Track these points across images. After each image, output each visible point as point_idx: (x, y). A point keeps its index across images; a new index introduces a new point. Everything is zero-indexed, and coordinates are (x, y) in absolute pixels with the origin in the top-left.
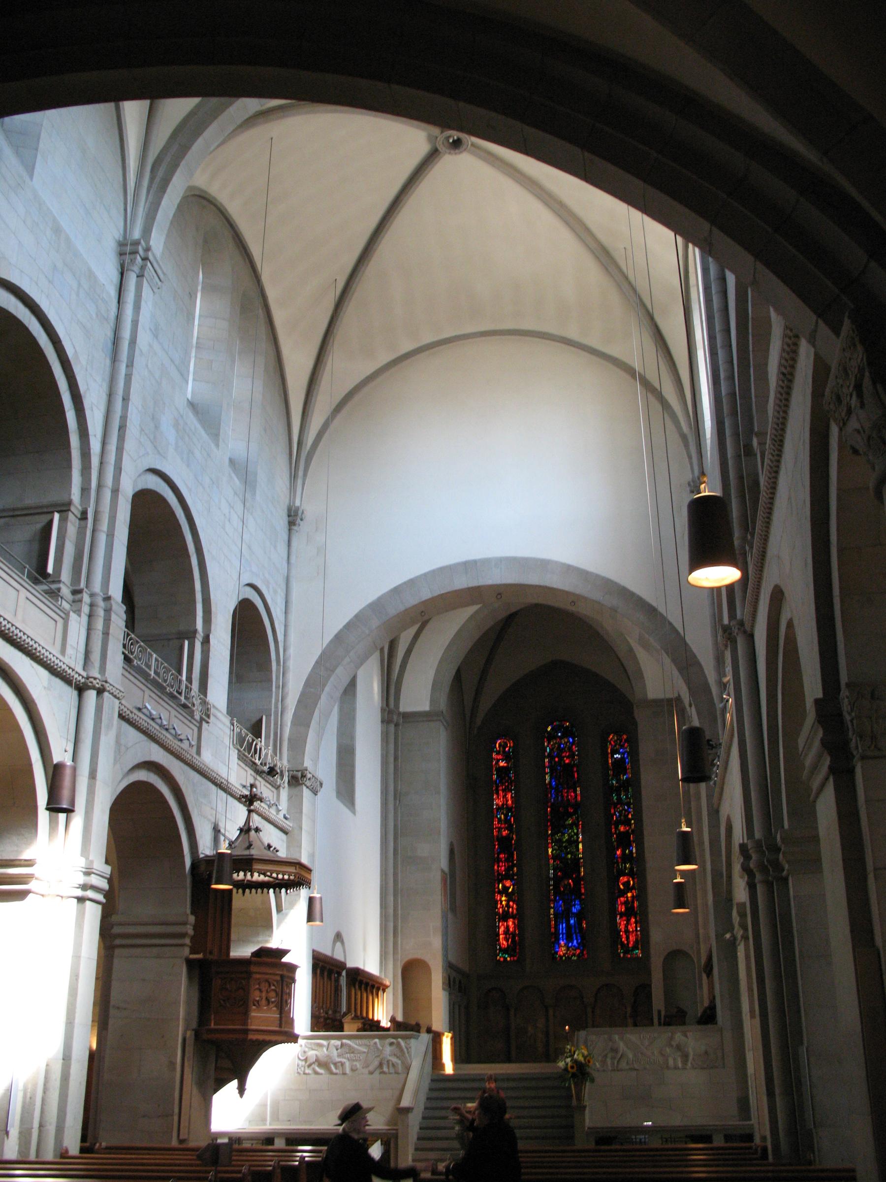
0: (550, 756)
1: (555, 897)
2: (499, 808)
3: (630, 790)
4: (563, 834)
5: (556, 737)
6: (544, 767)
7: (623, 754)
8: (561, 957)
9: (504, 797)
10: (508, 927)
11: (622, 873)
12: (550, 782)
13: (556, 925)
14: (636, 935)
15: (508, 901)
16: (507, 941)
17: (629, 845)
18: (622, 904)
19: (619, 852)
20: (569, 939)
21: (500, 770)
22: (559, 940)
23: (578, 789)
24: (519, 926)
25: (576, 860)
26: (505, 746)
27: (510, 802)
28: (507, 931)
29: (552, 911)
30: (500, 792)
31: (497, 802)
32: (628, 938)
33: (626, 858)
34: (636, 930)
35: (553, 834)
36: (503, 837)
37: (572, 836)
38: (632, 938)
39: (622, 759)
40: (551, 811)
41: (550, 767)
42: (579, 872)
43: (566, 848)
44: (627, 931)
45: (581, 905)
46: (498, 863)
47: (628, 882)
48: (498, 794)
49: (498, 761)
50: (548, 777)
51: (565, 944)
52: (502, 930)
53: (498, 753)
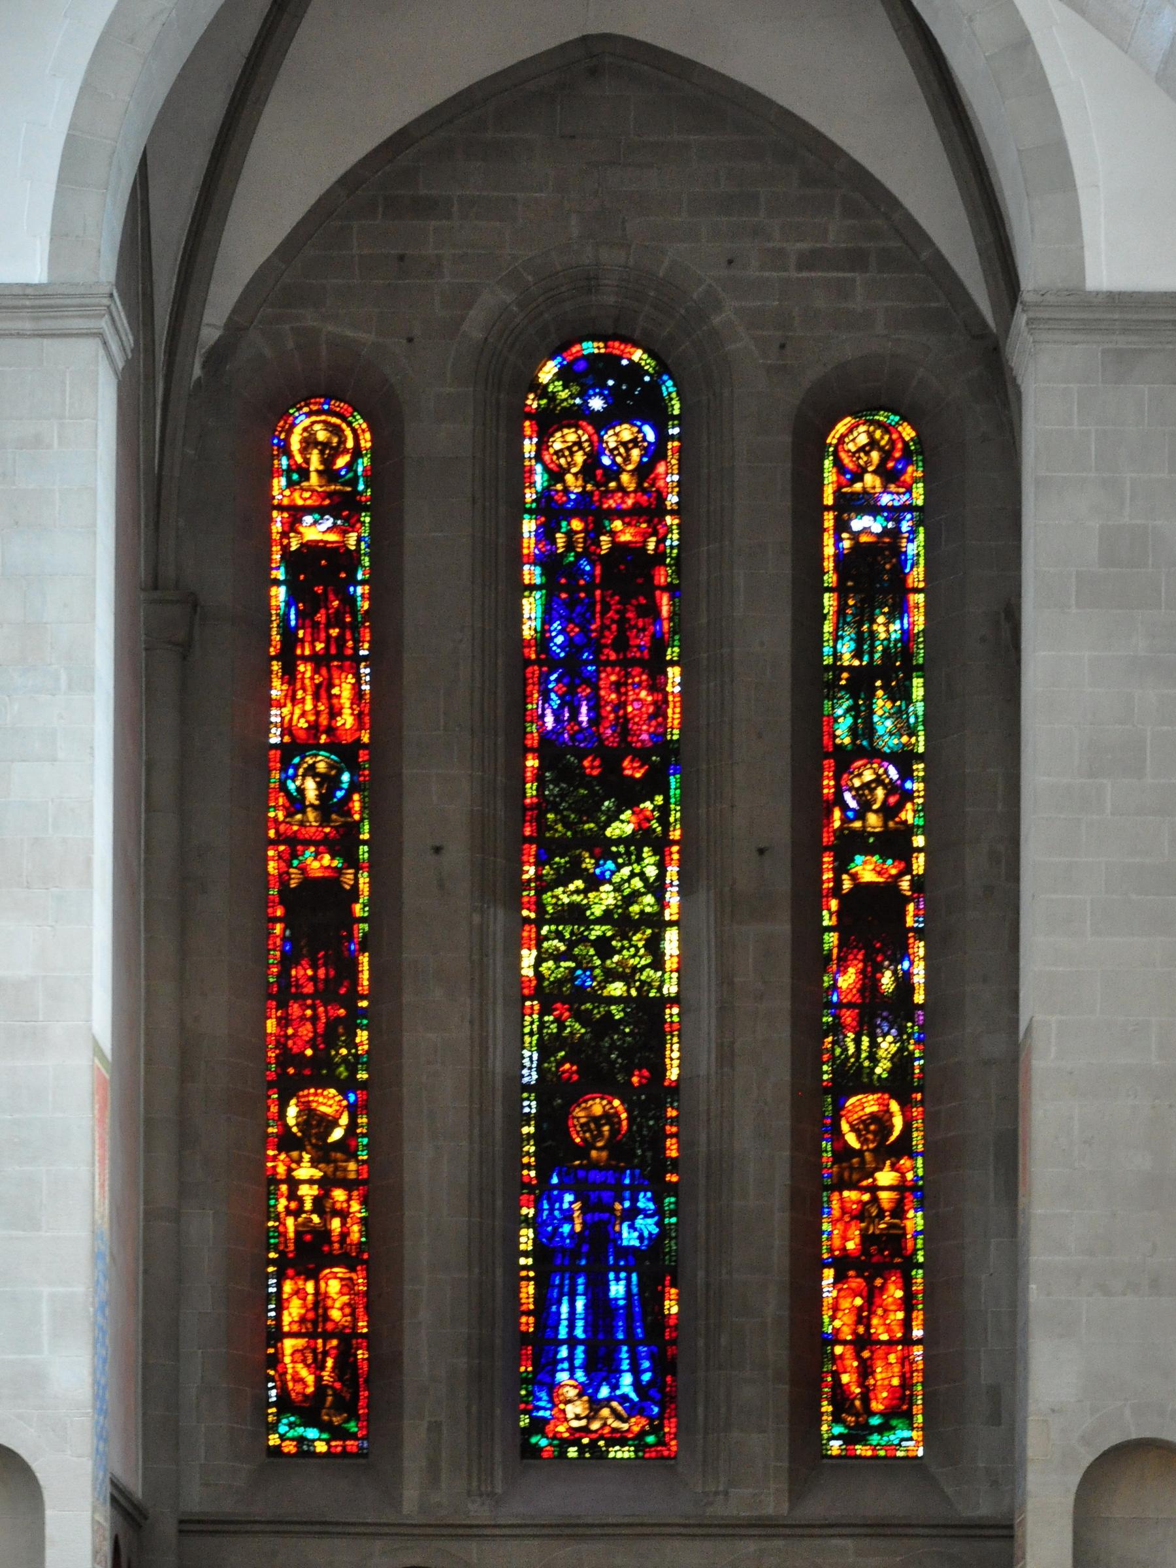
1: (544, 1176)
3: (918, 692)
4: (594, 882)
5: (575, 416)
6: (517, 560)
9: (323, 691)
10: (321, 1299)
11: (853, 1079)
12: (543, 640)
15: (325, 1185)
16: (317, 1366)
19: (848, 980)
20: (601, 1368)
22: (552, 1365)
23: (674, 673)
24: (376, 1301)
25: (647, 1010)
27: (347, 720)
28: (316, 1321)
29: (526, 1239)
31: (287, 713)
32: (865, 1371)
33: (875, 1010)
34: (908, 1341)
36: (309, 882)
37: (634, 896)
38: (886, 1375)
41: (548, 561)
43: (604, 947)
45: (659, 1212)
47: (881, 1121)
48: (289, 675)
49: (296, 514)
50: (532, 607)
52: (294, 1311)
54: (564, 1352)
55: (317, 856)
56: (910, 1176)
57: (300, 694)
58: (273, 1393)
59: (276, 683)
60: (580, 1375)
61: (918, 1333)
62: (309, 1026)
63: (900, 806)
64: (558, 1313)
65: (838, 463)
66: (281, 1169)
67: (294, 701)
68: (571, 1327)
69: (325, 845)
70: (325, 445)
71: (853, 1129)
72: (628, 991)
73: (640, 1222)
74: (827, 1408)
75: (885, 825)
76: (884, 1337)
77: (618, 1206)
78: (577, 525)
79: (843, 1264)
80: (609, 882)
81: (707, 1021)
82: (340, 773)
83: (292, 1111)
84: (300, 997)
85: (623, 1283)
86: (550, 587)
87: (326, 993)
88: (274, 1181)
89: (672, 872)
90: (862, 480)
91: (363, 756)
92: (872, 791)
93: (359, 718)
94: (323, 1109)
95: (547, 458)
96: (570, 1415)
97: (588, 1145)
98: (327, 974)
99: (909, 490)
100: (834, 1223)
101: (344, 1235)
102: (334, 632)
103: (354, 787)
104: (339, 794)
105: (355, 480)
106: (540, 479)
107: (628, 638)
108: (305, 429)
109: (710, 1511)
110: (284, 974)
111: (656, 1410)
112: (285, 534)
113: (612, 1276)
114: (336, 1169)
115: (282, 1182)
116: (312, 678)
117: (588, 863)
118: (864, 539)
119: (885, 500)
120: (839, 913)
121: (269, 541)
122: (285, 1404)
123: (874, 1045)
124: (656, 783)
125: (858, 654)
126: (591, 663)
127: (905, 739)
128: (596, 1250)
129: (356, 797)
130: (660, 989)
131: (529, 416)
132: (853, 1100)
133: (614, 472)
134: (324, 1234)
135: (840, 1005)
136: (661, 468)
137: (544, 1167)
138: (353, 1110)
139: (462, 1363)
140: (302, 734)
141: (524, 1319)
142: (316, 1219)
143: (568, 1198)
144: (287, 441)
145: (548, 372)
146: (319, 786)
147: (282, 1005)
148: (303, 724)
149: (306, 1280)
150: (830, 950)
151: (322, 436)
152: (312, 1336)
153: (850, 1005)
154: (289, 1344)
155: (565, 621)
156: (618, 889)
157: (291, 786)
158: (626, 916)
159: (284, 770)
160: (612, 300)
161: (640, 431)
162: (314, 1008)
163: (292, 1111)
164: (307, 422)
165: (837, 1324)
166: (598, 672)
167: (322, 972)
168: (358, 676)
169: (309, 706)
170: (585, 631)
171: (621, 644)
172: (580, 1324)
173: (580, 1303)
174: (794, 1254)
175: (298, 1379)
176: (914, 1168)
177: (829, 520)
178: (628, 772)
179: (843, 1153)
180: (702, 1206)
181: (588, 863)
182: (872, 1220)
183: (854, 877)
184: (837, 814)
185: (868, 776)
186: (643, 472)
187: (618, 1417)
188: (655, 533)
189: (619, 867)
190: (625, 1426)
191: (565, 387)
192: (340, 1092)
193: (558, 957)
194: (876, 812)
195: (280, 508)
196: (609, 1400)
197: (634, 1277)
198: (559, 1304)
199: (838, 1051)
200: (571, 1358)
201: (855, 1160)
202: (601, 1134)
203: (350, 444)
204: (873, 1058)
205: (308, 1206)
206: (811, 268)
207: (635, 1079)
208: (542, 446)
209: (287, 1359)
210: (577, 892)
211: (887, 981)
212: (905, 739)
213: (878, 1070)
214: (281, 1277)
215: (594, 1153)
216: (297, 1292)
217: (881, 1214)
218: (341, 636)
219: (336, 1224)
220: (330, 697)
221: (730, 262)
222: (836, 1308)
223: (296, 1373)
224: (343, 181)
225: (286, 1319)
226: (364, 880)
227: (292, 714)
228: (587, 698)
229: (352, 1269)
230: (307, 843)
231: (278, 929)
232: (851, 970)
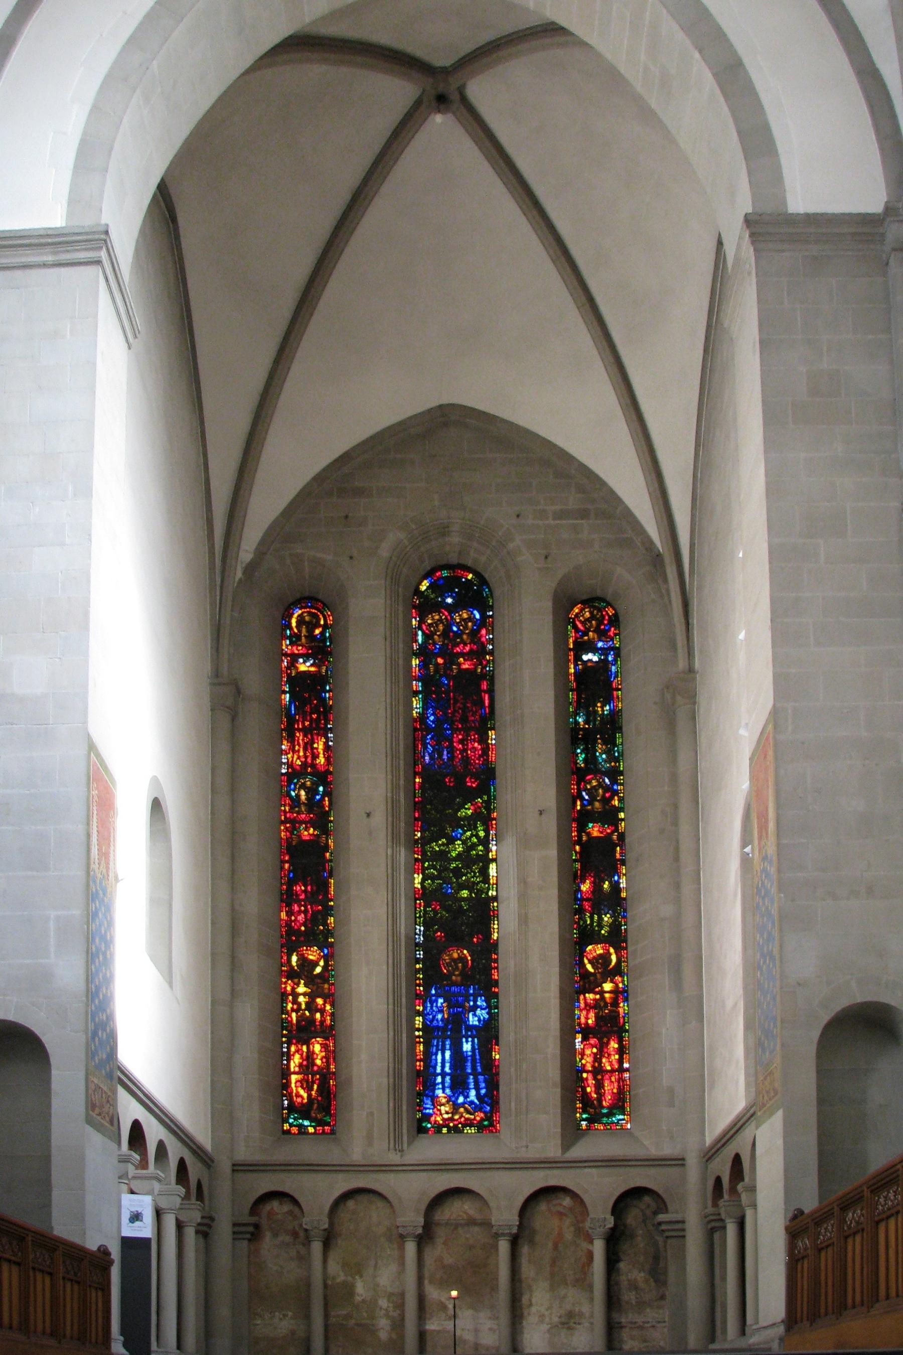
0: (424, 653)
1: (427, 990)
2: (294, 774)
4: (451, 840)
5: (439, 607)
8: (438, 1128)
9: (309, 746)
11: (587, 936)
12: (423, 717)
13: (428, 1056)
14: (620, 1080)
15: (312, 996)
16: (309, 1089)
18: (588, 1007)
20: (459, 1086)
21: (299, 682)
27: (321, 760)
29: (419, 1021)
32: (599, 1086)
34: (621, 1070)
35: (425, 841)
36: (302, 842)
37: (474, 846)
38: (610, 1087)
39: (603, 665)
40: (422, 785)
43: (457, 872)
44: (598, 1071)
45: (489, 1007)
46: (289, 905)
47: (606, 957)
48: (292, 739)
49: (294, 658)
51: (449, 1099)
53: (295, 639)
54: (439, 1079)
55: (306, 829)
56: (621, 985)
57: (297, 748)
58: (286, 1102)
59: (285, 742)
60: (448, 1091)
61: (626, 1065)
62: (303, 915)
63: (612, 798)
64: (436, 1060)
65: (575, 627)
66: (289, 988)
67: (294, 752)
68: (443, 1066)
69: (309, 823)
71: (590, 962)
72: (471, 894)
73: (478, 1012)
75: (604, 807)
76: (609, 1068)
77: (467, 1004)
78: (440, 661)
79: (587, 1032)
80: (460, 840)
82: (318, 786)
83: (294, 959)
84: (298, 902)
85: (470, 1043)
88: (284, 995)
90: (587, 635)
92: (597, 790)
93: (328, 759)
94: (311, 957)
95: (424, 627)
96: (443, 1112)
97: (450, 974)
98: (312, 888)
99: (612, 640)
100: (581, 1010)
101: (323, 1021)
102: (314, 716)
104: (318, 797)
105: (324, 641)
106: (420, 638)
107: (467, 717)
108: (299, 616)
111: (489, 1108)
112: (288, 668)
113: (464, 1040)
114: (318, 987)
115: (290, 995)
116: (303, 740)
117: (449, 830)
118: (589, 664)
119: (600, 644)
120: (581, 853)
123: (600, 919)
125: (587, 722)
126: (449, 729)
127: (613, 764)
128: (456, 1027)
129: (327, 799)
130: (487, 893)
132: (590, 947)
134: (312, 1020)
135: (582, 899)
136: (484, 632)
138: (327, 958)
140: (298, 768)
141: (418, 1063)
142: (307, 1013)
143: (441, 1001)
144: (290, 623)
145: (424, 586)
146: (307, 794)
147: (289, 905)
149: (302, 1045)
150: (576, 872)
153: (587, 900)
154: (294, 1078)
157: (293, 794)
161: (472, 613)
162: (305, 906)
163: (294, 959)
164: (300, 612)
165: (583, 1062)
166: (452, 734)
167: (309, 888)
168: (327, 739)
169: (301, 754)
170: (445, 714)
171: (464, 720)
172: (447, 1065)
173: (448, 1054)
175: (298, 1095)
176: (623, 982)
178: (469, 784)
179: (585, 974)
182: (601, 1008)
183: (588, 834)
184: (579, 803)
185: (594, 783)
187: (468, 1112)
188: (481, 664)
189: (465, 832)
190: (472, 1117)
191: (432, 593)
192: (319, 948)
193: (433, 878)
194: (598, 801)
195: (286, 655)
196: (464, 1103)
197: (476, 1040)
198: (436, 1054)
199: (581, 923)
200: (443, 1083)
201: (592, 978)
202: (457, 968)
203: (322, 622)
204: (601, 926)
205: (303, 1006)
206: (560, 518)
207: (475, 940)
208: (421, 622)
209: (293, 1085)
210: (443, 844)
211: (606, 885)
212: (613, 764)
213: (603, 932)
215: (454, 978)
216: (297, 1051)
217: (606, 1004)
218: (318, 718)
219: (318, 1016)
220: (313, 748)
221: (518, 516)
222: (583, 1054)
223: (297, 1092)
224: (314, 479)
225: (292, 1065)
227: (293, 757)
228: (447, 748)
229: (327, 1039)
230: (301, 823)
231: (287, 866)
232: (588, 881)
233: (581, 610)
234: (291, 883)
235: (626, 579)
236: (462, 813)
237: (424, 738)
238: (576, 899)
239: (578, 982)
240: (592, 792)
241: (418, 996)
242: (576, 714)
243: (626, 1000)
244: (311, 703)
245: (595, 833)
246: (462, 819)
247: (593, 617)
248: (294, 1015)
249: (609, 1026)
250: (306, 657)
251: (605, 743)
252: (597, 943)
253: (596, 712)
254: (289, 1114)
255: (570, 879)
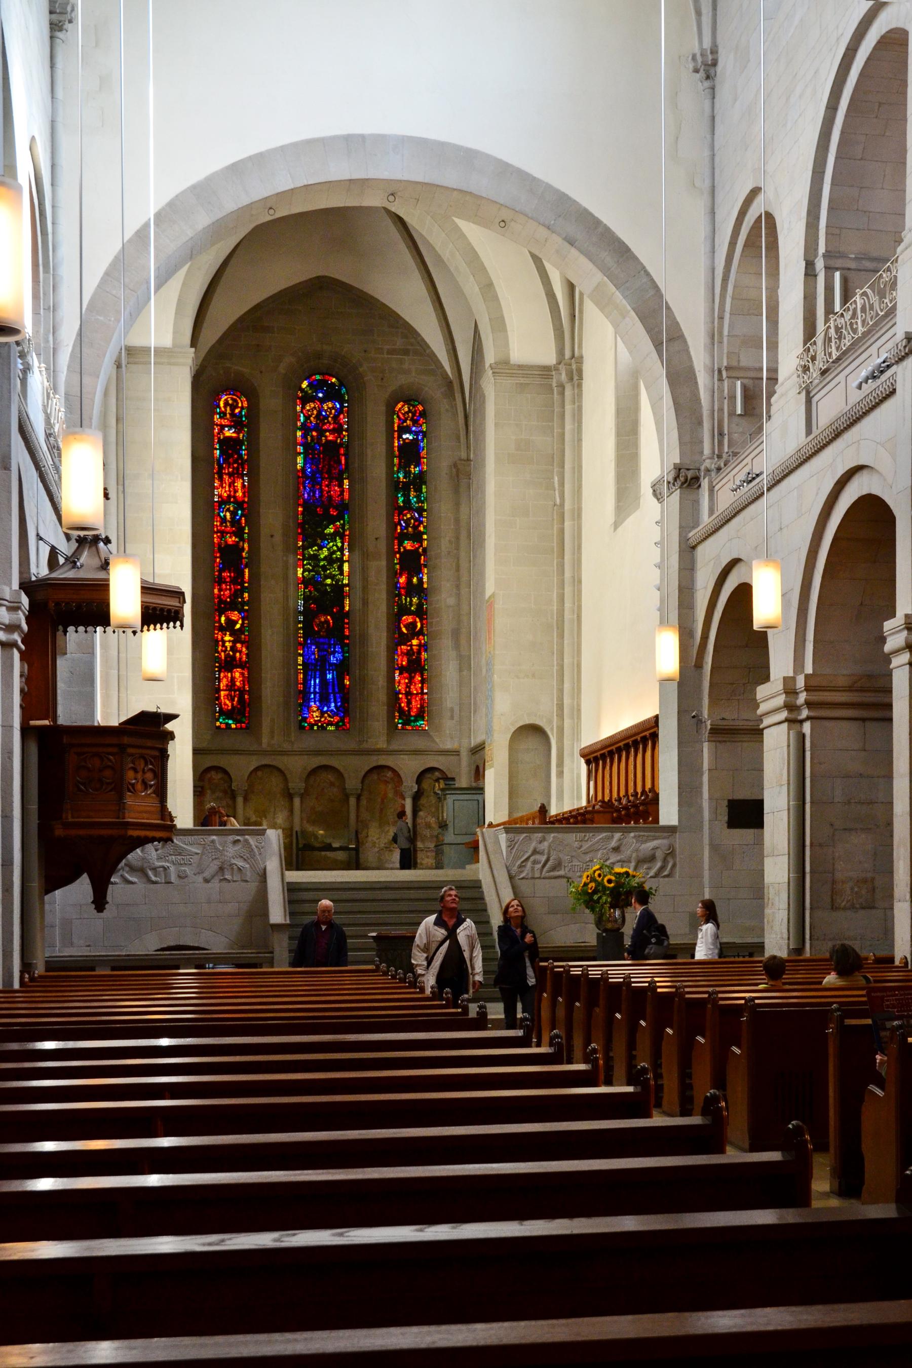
0: (305, 428)
2: (223, 502)
4: (321, 548)
5: (314, 399)
7: (416, 433)
8: (311, 726)
9: (231, 484)
10: (233, 679)
11: (404, 610)
12: (303, 469)
14: (422, 699)
15: (234, 642)
16: (232, 700)
17: (418, 571)
19: (402, 580)
20: (324, 701)
21: (226, 443)
22: (309, 700)
23: (346, 482)
25: (338, 588)
26: (233, 407)
27: (240, 494)
29: (300, 659)
30: (226, 477)
32: (409, 703)
34: (422, 693)
35: (304, 548)
36: (227, 545)
37: (334, 552)
39: (415, 442)
40: (303, 513)
42: (344, 607)
43: (324, 568)
44: (408, 694)
45: (343, 652)
47: (414, 624)
48: (221, 479)
49: (222, 427)
53: (223, 415)
55: (231, 537)
61: (425, 691)
63: (419, 526)
65: (398, 416)
66: (220, 637)
68: (315, 688)
70: (231, 406)
74: (397, 714)
78: (314, 434)
79: (402, 669)
81: (359, 593)
83: (223, 619)
84: (225, 582)
86: (306, 453)
87: (234, 581)
88: (217, 641)
89: (346, 544)
91: (245, 506)
93: (244, 493)
101: (241, 658)
102: (235, 465)
103: (242, 515)
105: (242, 416)
106: (302, 419)
109: (361, 747)
110: (220, 574)
112: (218, 433)
117: (319, 541)
119: (414, 429)
121: (214, 436)
122: (222, 712)
123: (411, 601)
124: (340, 517)
125: (404, 477)
131: (299, 398)
133: (327, 417)
134: (234, 657)
135: (400, 588)
136: (342, 416)
137: (305, 637)
138: (243, 619)
139: (281, 699)
145: (305, 384)
147: (220, 585)
148: (225, 495)
151: (230, 402)
152: (230, 690)
154: (222, 693)
155: (311, 464)
156: (329, 549)
157: (222, 514)
158: (331, 558)
159: (219, 509)
160: (326, 362)
163: (223, 619)
168: (244, 480)
170: (318, 467)
171: (329, 472)
173: (317, 681)
174: (388, 666)
175: (225, 704)
177: (396, 435)
180: (357, 650)
181: (319, 541)
183: (404, 548)
185: (409, 516)
186: (336, 418)
193: (309, 571)
195: (217, 425)
200: (315, 698)
204: (411, 605)
208: (303, 408)
211: (415, 580)
214: (220, 672)
216: (225, 676)
217: (414, 653)
219: (238, 655)
222: (399, 682)
225: (222, 685)
226: (246, 545)
229: (243, 669)
230: (227, 533)
233: (403, 406)
234: (221, 571)
235: (432, 390)
236: (327, 531)
237: (304, 483)
238: (397, 587)
239: (398, 639)
240: (407, 522)
241: (300, 643)
242: (398, 472)
243: (426, 651)
244: (233, 457)
245: (409, 548)
246: (326, 535)
247: (410, 411)
248: (223, 654)
249: (415, 667)
250: (230, 427)
251: (415, 491)
252: (409, 615)
253: (410, 471)
254: (219, 716)
255: (393, 575)
